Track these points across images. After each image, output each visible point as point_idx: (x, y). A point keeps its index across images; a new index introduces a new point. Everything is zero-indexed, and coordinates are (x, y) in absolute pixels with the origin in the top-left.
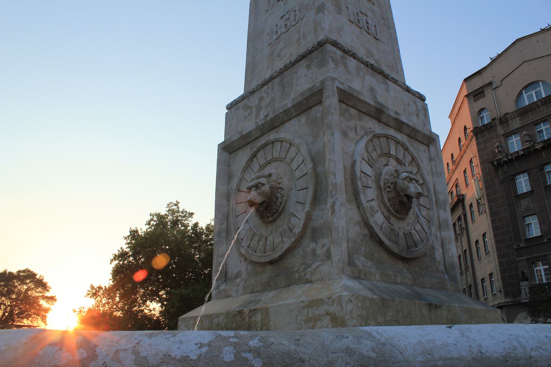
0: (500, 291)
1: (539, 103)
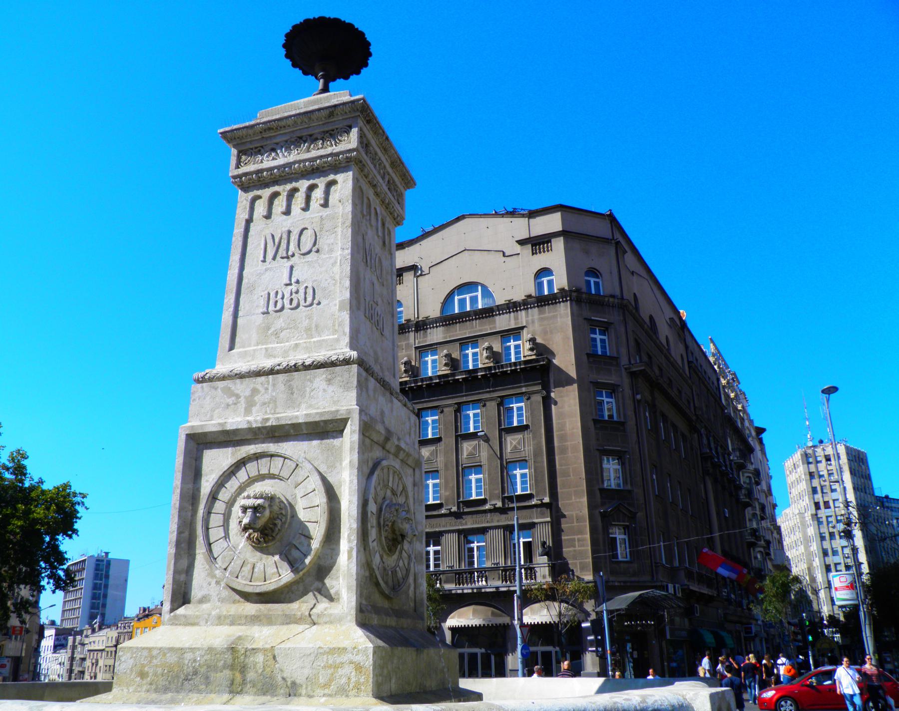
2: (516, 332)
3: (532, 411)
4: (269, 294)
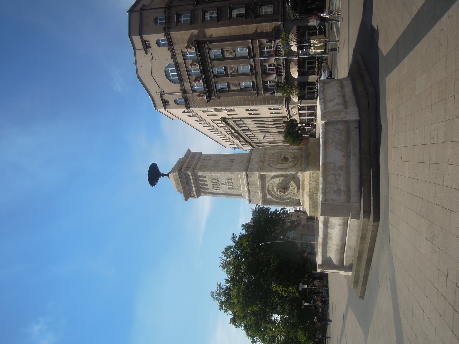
0: (279, 106)
1: (177, 72)
2: (184, 54)
3: (215, 48)
4: (228, 189)
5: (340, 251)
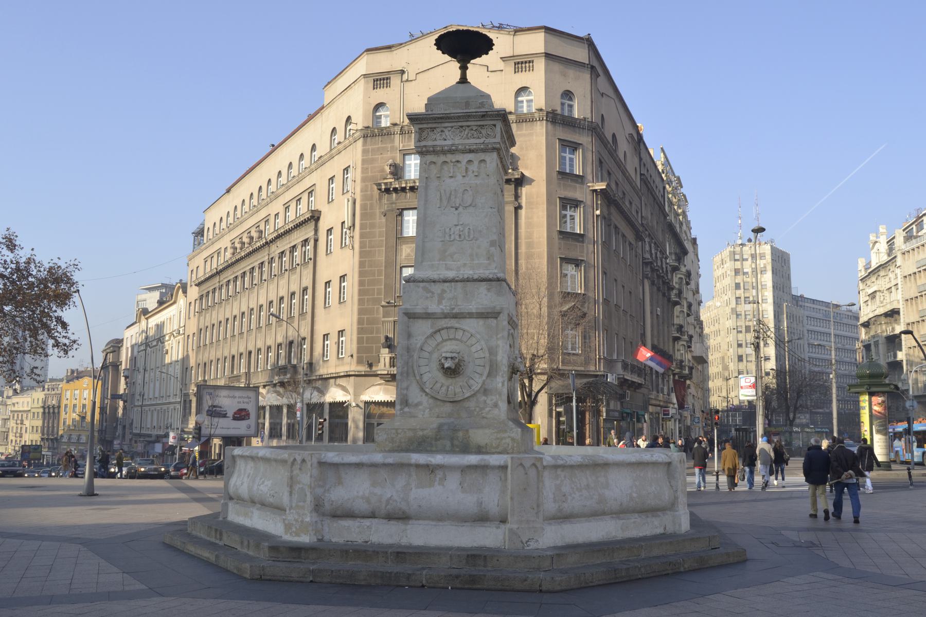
5: (384, 505)
